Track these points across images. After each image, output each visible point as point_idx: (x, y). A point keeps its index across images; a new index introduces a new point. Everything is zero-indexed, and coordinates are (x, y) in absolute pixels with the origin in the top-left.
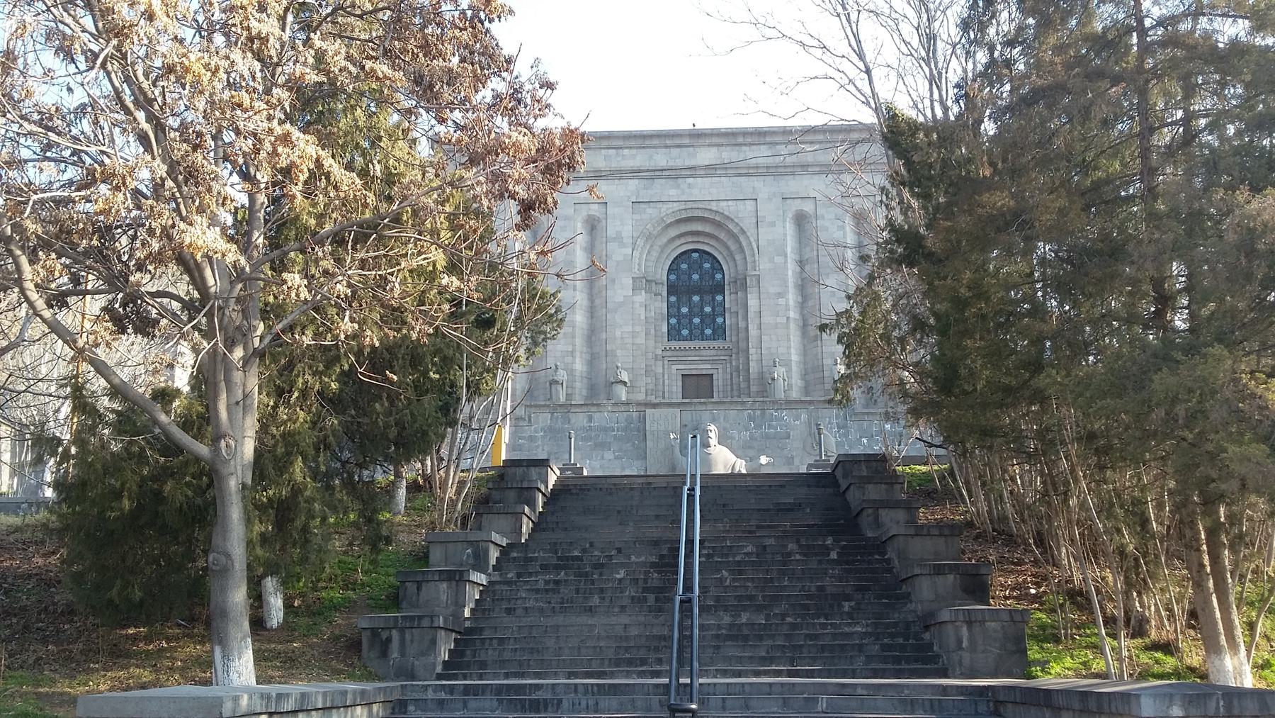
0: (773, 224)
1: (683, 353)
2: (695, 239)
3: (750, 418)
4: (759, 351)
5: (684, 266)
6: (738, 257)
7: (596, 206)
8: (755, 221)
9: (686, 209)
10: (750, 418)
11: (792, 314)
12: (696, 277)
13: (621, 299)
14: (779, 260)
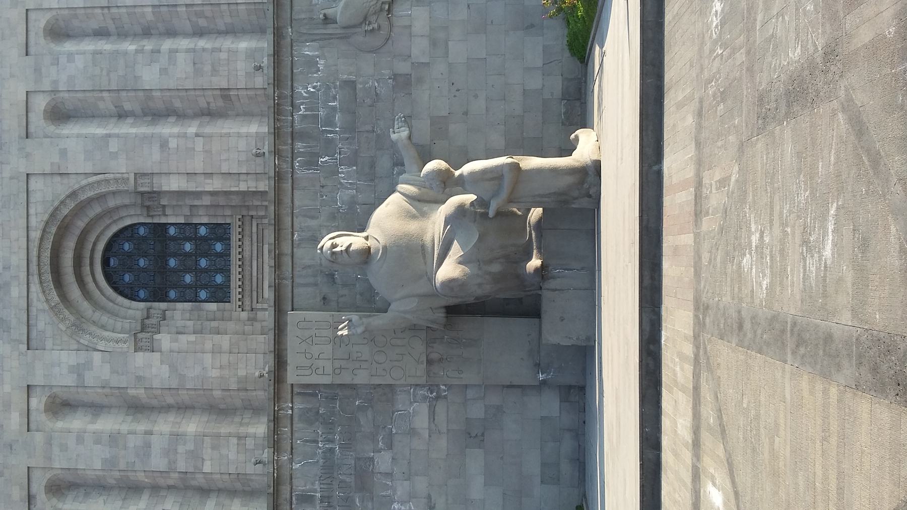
0: (63, 153)
1: (247, 283)
2: (87, 261)
3: (311, 162)
4: (242, 177)
5: (127, 278)
6: (112, 203)
7: (34, 402)
8: (57, 179)
9: (40, 275)
10: (311, 162)
11: (192, 130)
12: (142, 263)
13: (165, 369)
14: (114, 146)
